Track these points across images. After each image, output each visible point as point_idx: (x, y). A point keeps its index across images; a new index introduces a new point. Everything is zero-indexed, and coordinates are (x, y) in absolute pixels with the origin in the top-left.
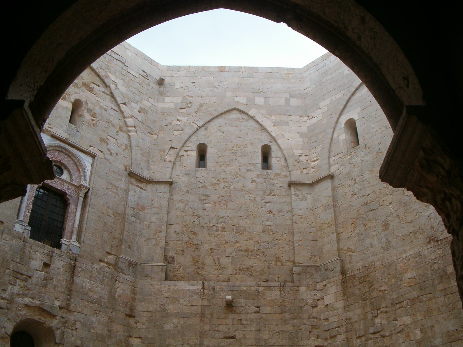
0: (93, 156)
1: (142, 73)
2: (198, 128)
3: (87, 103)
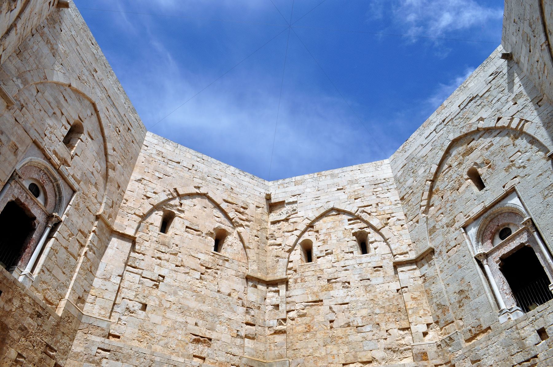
0: (513, 190)
1: (492, 77)
2: (547, 43)
3: (476, 164)
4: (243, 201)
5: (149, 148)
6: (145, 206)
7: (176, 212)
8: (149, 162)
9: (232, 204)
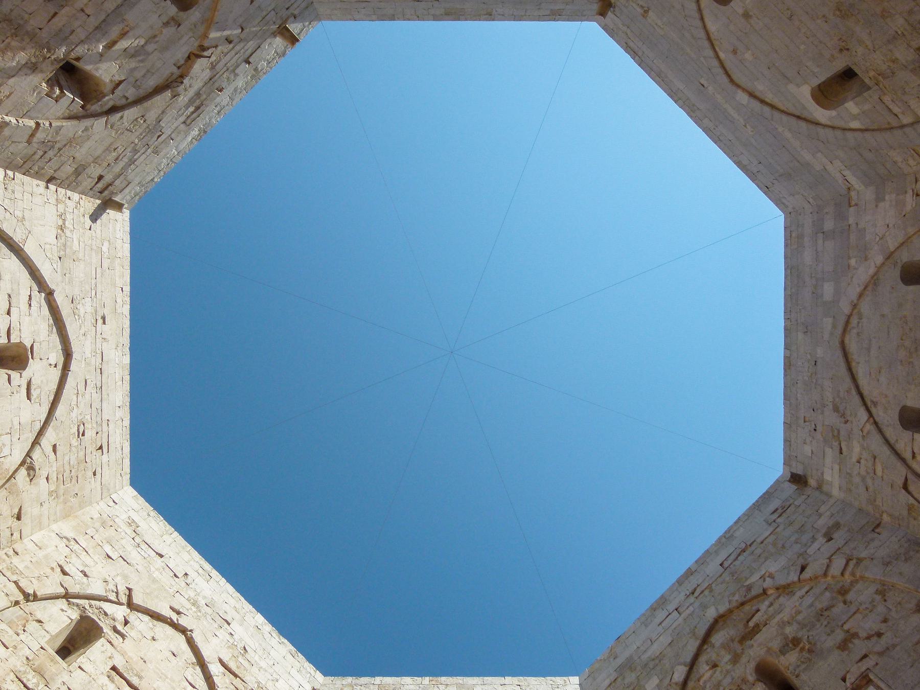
4: (259, 683)
5: (116, 507)
6: (48, 582)
7: (107, 630)
8: (103, 524)
9: (236, 676)
